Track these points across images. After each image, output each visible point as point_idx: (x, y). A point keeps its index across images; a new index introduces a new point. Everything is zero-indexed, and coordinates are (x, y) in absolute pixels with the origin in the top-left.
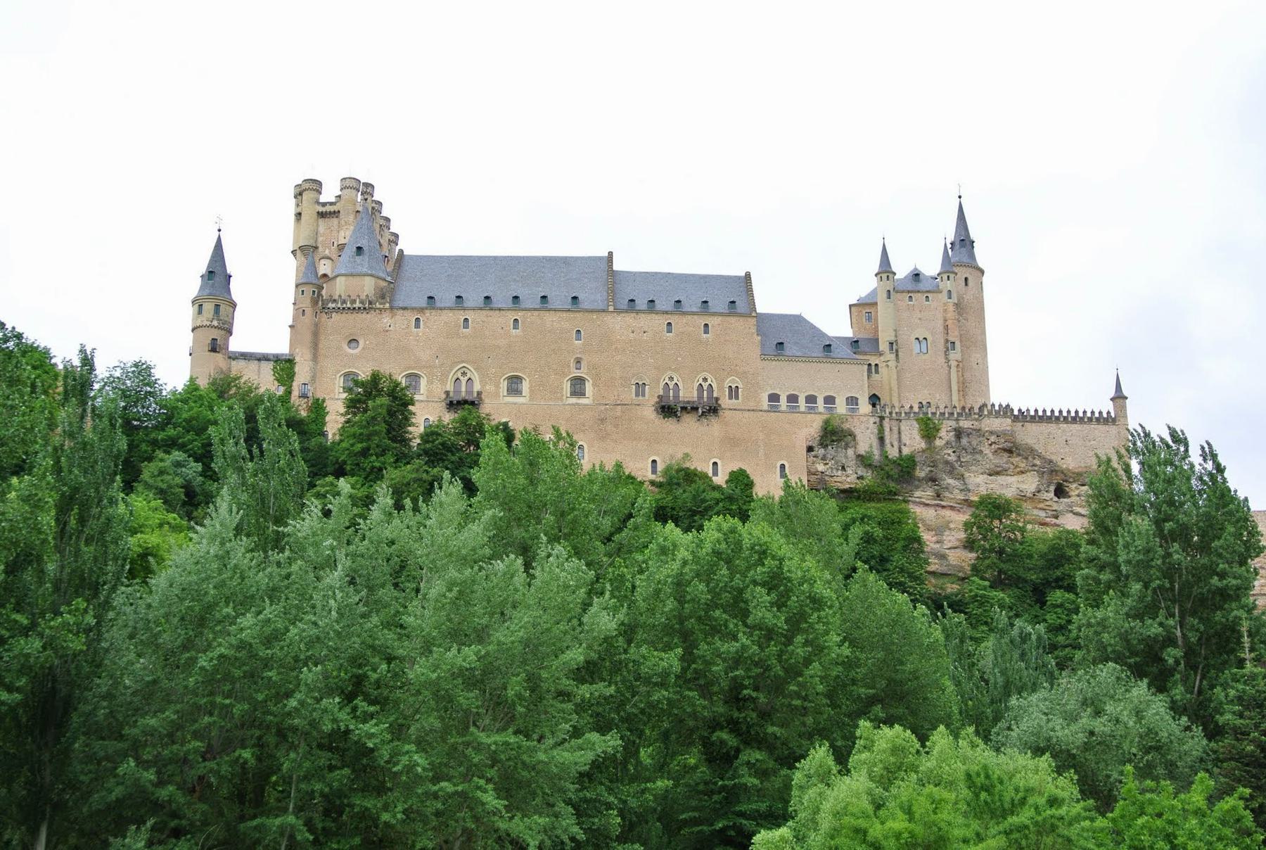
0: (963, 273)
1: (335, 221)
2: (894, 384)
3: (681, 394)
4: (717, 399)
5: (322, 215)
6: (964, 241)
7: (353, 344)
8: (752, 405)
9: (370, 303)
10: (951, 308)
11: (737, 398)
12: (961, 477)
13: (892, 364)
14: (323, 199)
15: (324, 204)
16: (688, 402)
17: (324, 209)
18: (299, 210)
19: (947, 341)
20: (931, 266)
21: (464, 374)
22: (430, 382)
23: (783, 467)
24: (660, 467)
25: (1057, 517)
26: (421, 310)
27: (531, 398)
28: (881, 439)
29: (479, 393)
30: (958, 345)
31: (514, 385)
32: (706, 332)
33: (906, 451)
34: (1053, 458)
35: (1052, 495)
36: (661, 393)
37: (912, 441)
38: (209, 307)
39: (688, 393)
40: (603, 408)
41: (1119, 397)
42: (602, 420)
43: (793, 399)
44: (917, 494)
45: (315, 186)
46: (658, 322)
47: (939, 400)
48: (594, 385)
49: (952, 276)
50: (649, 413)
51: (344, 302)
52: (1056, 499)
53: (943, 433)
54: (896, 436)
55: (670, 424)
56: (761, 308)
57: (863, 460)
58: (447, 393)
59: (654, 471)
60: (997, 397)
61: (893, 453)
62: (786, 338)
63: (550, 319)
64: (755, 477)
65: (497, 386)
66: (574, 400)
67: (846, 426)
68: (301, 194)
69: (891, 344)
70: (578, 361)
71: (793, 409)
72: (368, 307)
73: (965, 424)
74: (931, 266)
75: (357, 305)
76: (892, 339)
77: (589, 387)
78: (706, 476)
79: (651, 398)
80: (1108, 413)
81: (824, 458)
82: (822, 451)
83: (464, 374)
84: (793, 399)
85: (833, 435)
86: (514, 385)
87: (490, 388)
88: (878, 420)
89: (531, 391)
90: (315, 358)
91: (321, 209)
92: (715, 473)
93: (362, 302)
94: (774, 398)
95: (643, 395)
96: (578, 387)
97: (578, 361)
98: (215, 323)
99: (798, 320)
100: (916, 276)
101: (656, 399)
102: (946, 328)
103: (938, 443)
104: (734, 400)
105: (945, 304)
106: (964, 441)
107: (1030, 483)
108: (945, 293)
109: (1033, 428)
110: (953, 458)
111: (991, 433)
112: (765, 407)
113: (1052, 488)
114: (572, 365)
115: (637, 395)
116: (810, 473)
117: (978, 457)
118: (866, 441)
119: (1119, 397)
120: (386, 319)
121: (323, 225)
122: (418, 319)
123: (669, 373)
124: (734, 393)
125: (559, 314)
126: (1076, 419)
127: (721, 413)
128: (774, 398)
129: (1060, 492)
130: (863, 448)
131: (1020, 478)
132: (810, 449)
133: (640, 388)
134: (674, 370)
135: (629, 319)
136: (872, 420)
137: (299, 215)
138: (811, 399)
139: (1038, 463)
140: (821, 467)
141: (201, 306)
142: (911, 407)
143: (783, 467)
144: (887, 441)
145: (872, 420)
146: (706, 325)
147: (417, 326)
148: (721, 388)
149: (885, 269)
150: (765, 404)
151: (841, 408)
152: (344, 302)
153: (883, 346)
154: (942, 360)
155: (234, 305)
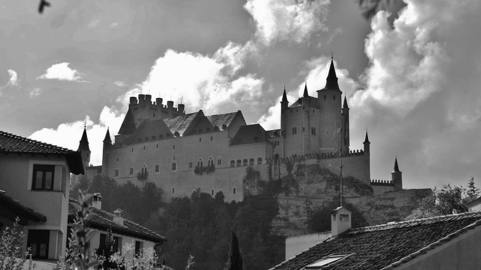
3: (203, 165)
12: (297, 187)
21: (144, 166)
23: (234, 189)
33: (281, 177)
36: (197, 165)
37: (284, 171)
39: (205, 165)
41: (367, 143)
44: (280, 195)
50: (193, 173)
52: (335, 191)
54: (278, 171)
55: (199, 177)
57: (261, 183)
64: (225, 194)
66: (173, 171)
71: (239, 166)
73: (302, 163)
78: (209, 195)
79: (194, 169)
81: (247, 184)
84: (239, 161)
85: (252, 174)
88: (269, 166)
92: (213, 194)
94: (233, 162)
103: (293, 172)
104: (219, 165)
112: (229, 166)
116: (245, 190)
117: (302, 177)
124: (219, 162)
128: (233, 162)
132: (244, 181)
133: (191, 165)
136: (267, 166)
138: (245, 161)
139: (328, 176)
140: (247, 188)
143: (234, 189)
144: (273, 174)
145: (267, 166)
150: (229, 164)
151: (256, 163)
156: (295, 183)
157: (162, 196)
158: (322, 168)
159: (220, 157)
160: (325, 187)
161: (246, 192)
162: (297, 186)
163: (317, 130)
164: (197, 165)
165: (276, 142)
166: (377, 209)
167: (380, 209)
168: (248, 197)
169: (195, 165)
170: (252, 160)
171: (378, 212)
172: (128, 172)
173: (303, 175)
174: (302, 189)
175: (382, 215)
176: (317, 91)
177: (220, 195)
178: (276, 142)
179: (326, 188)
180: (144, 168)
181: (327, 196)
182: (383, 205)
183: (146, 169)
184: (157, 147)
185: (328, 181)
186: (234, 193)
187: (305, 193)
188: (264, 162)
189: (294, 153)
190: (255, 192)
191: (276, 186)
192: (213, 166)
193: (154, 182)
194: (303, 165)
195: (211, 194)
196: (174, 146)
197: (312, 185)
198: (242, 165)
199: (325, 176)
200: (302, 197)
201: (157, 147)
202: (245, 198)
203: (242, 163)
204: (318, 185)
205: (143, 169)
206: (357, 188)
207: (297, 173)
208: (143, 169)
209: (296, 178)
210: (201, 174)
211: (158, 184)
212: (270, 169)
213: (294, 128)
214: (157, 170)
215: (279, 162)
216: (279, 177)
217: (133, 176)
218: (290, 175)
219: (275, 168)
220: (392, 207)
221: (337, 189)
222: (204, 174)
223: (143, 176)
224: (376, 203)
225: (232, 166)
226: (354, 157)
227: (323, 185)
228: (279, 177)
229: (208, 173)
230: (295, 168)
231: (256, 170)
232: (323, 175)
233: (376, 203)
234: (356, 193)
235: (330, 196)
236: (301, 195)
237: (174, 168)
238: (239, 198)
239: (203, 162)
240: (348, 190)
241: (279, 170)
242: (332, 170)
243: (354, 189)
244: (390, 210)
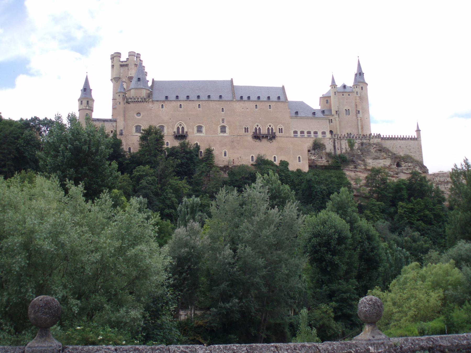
0: (361, 85)
1: (127, 68)
2: (338, 127)
4: (275, 133)
5: (122, 66)
6: (360, 74)
7: (139, 115)
8: (287, 135)
9: (145, 99)
10: (358, 98)
11: (282, 132)
13: (337, 119)
14: (121, 60)
15: (122, 62)
16: (264, 134)
17: (122, 64)
18: (113, 64)
19: (357, 110)
20: (350, 83)
21: (180, 125)
22: (168, 128)
23: (299, 158)
24: (255, 159)
25: (397, 174)
26: (164, 101)
27: (206, 134)
28: (335, 147)
29: (187, 132)
30: (361, 112)
31: (199, 129)
32: (270, 108)
34: (395, 152)
35: (395, 166)
38: (85, 102)
39: (264, 131)
40: (233, 137)
41: (418, 131)
42: (233, 142)
43: (302, 132)
45: (118, 55)
46: (253, 105)
47: (354, 132)
48: (229, 128)
49: (358, 86)
50: (250, 138)
51: (135, 99)
53: (356, 145)
54: (339, 146)
55: (258, 143)
56: (290, 98)
57: (329, 155)
58: (174, 132)
59: (252, 160)
60: (375, 129)
61: (338, 152)
62: (298, 111)
63: (212, 104)
65: (193, 129)
66: (222, 134)
67: (322, 142)
68: (113, 58)
69: (336, 112)
70: (223, 120)
71: (302, 137)
72: (144, 100)
73: (365, 141)
74: (350, 83)
75: (140, 100)
76: (337, 110)
78: (272, 162)
81: (314, 154)
82: (313, 152)
83: (180, 125)
84: (302, 132)
85: (317, 146)
86: (199, 129)
87: (190, 130)
89: (206, 131)
90: (125, 120)
91: (121, 64)
92: (275, 160)
93: (141, 99)
94: (295, 132)
95: (248, 132)
96: (223, 129)
97: (223, 120)
98: (87, 108)
99: (302, 102)
100: (344, 87)
101: (252, 133)
102: (356, 105)
104: (281, 133)
105: (356, 97)
106: (364, 146)
107: (388, 162)
108: (355, 93)
110: (360, 153)
111: (374, 144)
112: (292, 136)
113: (395, 164)
115: (245, 132)
116: (309, 160)
118: (329, 148)
119: (418, 131)
120: (151, 105)
121: (122, 69)
122: (162, 105)
123: (257, 124)
124: (281, 131)
125: (215, 102)
126: (403, 139)
127: (276, 138)
128: (295, 132)
129: (398, 165)
130: (328, 150)
131: (384, 160)
132: (309, 151)
133: (246, 130)
135: (241, 104)
137: (113, 66)
138: (309, 133)
139: (390, 154)
140: (313, 158)
141: (82, 101)
142: (345, 135)
143: (299, 158)
144: (337, 148)
146: (270, 106)
148: (276, 129)
149: (333, 85)
150: (292, 135)
152: (135, 99)
153: (334, 112)
154: (355, 117)
155: (93, 101)
169: (251, 131)
170: (316, 133)
180: (180, 128)
183: (183, 128)
186: (300, 161)
189: (349, 131)
190: (323, 162)
193: (197, 143)
196: (223, 109)
197: (378, 161)
198: (306, 136)
200: (369, 170)
203: (306, 134)
205: (178, 128)
208: (178, 128)
212: (334, 143)
216: (341, 152)
225: (296, 136)
230: (356, 146)
236: (368, 168)
239: (261, 129)
241: (341, 145)
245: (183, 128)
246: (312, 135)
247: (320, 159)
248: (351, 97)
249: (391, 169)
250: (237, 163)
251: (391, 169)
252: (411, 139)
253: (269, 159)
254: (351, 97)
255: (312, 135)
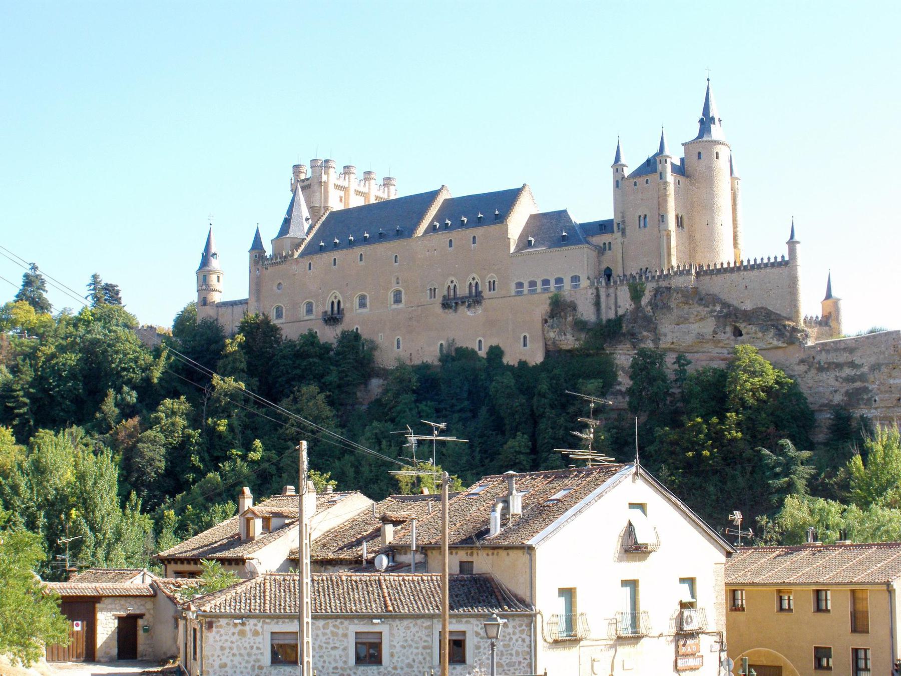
4: (481, 292)
13: (620, 240)
21: (336, 297)
22: (317, 306)
23: (525, 337)
27: (371, 310)
28: (597, 304)
33: (621, 312)
36: (446, 293)
37: (625, 303)
40: (410, 309)
41: (792, 243)
43: (533, 284)
44: (620, 347)
48: (406, 294)
50: (438, 309)
52: (733, 338)
53: (647, 292)
54: (612, 301)
55: (450, 315)
57: (580, 326)
58: (326, 312)
65: (352, 304)
66: (395, 306)
73: (664, 284)
75: (279, 260)
77: (403, 296)
78: (473, 352)
79: (439, 299)
80: (783, 257)
81: (552, 327)
82: (550, 321)
85: (559, 308)
90: (258, 300)
92: (480, 349)
94: (520, 285)
98: (204, 287)
109: (718, 279)
112: (513, 293)
114: (394, 280)
117: (664, 310)
119: (792, 243)
124: (492, 286)
127: (483, 302)
128: (520, 285)
131: (701, 324)
134: (453, 275)
136: (590, 291)
138: (546, 282)
140: (552, 335)
143: (525, 337)
144: (603, 305)
145: (590, 291)
147: (310, 269)
150: (513, 289)
151: (567, 285)
156: (649, 323)
157: (376, 353)
158: (704, 292)
159: (492, 276)
160: (712, 329)
161: (549, 343)
162: (656, 328)
163: (685, 220)
164: (446, 293)
165: (605, 244)
166: (821, 369)
167: (828, 369)
168: (552, 354)
169: (441, 292)
170: (559, 281)
171: (823, 376)
172: (303, 309)
173: (669, 308)
174: (665, 335)
175: (832, 382)
176: (683, 144)
177: (496, 353)
178: (605, 244)
179: (715, 332)
181: (716, 347)
182: (834, 363)
183: (339, 302)
184: (361, 260)
185: (718, 318)
186: (525, 345)
187: (673, 343)
188: (584, 283)
190: (569, 341)
191: (611, 331)
192: (479, 294)
194: (666, 288)
195: (477, 349)
198: (539, 290)
199: (711, 307)
201: (361, 260)
202: (548, 353)
204: (695, 328)
205: (333, 303)
206: (779, 330)
207: (653, 304)
208: (333, 303)
209: (651, 314)
210: (456, 310)
211: (365, 334)
212: (598, 296)
213: (642, 217)
214: (362, 305)
215: (615, 282)
216: (616, 312)
217: (312, 317)
218: (638, 308)
219: (608, 296)
220: (852, 365)
221: (738, 333)
222: (462, 309)
223: (333, 318)
224: (818, 358)
225: (519, 293)
226: (768, 270)
227: (708, 327)
228: (616, 312)
229: (469, 306)
231: (568, 299)
232: (708, 307)
233: (818, 358)
234: (778, 340)
235: (722, 347)
237: (398, 300)
238: (536, 357)
240: (760, 335)
241: (616, 298)
242: (724, 296)
243: (772, 331)
244: (847, 371)
245: (339, 302)
246: (552, 286)
247: (563, 338)
248: (671, 181)
249: (719, 341)
250: (417, 362)
251: (719, 341)
252: (773, 265)
253: (470, 346)
254: (671, 181)
255: (552, 286)
